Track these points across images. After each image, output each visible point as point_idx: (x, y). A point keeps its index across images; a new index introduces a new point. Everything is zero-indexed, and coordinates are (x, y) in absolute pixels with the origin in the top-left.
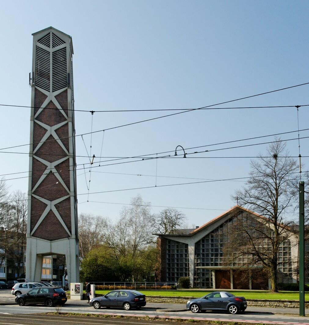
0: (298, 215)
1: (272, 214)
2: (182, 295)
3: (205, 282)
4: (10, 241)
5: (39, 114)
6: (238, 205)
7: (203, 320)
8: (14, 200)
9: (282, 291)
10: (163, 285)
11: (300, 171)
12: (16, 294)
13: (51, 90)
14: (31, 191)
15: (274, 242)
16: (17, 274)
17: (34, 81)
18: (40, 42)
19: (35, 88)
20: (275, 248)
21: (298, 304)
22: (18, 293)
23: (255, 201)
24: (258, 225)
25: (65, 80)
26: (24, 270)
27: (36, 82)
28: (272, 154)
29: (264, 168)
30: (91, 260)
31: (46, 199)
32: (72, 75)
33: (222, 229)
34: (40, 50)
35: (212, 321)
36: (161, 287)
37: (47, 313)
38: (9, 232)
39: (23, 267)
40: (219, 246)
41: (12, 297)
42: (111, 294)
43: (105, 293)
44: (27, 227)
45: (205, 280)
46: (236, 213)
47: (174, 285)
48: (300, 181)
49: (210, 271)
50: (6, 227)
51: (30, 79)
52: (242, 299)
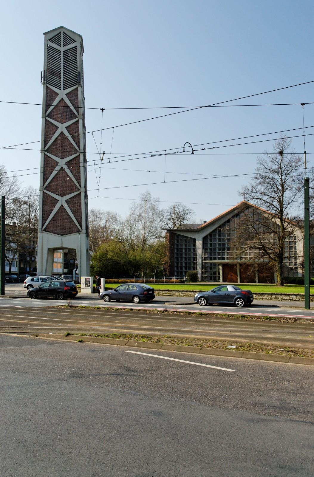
0: (304, 210)
1: (279, 210)
2: (190, 288)
3: (213, 276)
4: (22, 236)
5: (50, 113)
6: (244, 200)
7: (210, 313)
8: (26, 196)
9: (288, 285)
10: (171, 279)
11: (305, 167)
12: (28, 288)
13: (62, 88)
14: (42, 187)
15: (280, 237)
16: (29, 268)
17: (46, 79)
18: (51, 41)
19: (47, 86)
20: (280, 242)
21: (304, 297)
22: (30, 286)
23: (261, 196)
24: (264, 220)
25: (76, 78)
26: (35, 265)
27: (48, 81)
28: (278, 150)
29: (270, 164)
30: (101, 254)
31: (57, 195)
32: (83, 73)
33: (229, 224)
34: (51, 49)
35: (219, 314)
36: (170, 281)
37: (58, 306)
38: (22, 227)
39: (35, 262)
40: (226, 240)
41: (24, 291)
42: (120, 288)
43: (115, 286)
44: (39, 222)
45: (213, 274)
46: (243, 208)
47: (182, 278)
48: (305, 177)
49: (218, 265)
50: (18, 222)
51: (42, 77)
52: (248, 292)
